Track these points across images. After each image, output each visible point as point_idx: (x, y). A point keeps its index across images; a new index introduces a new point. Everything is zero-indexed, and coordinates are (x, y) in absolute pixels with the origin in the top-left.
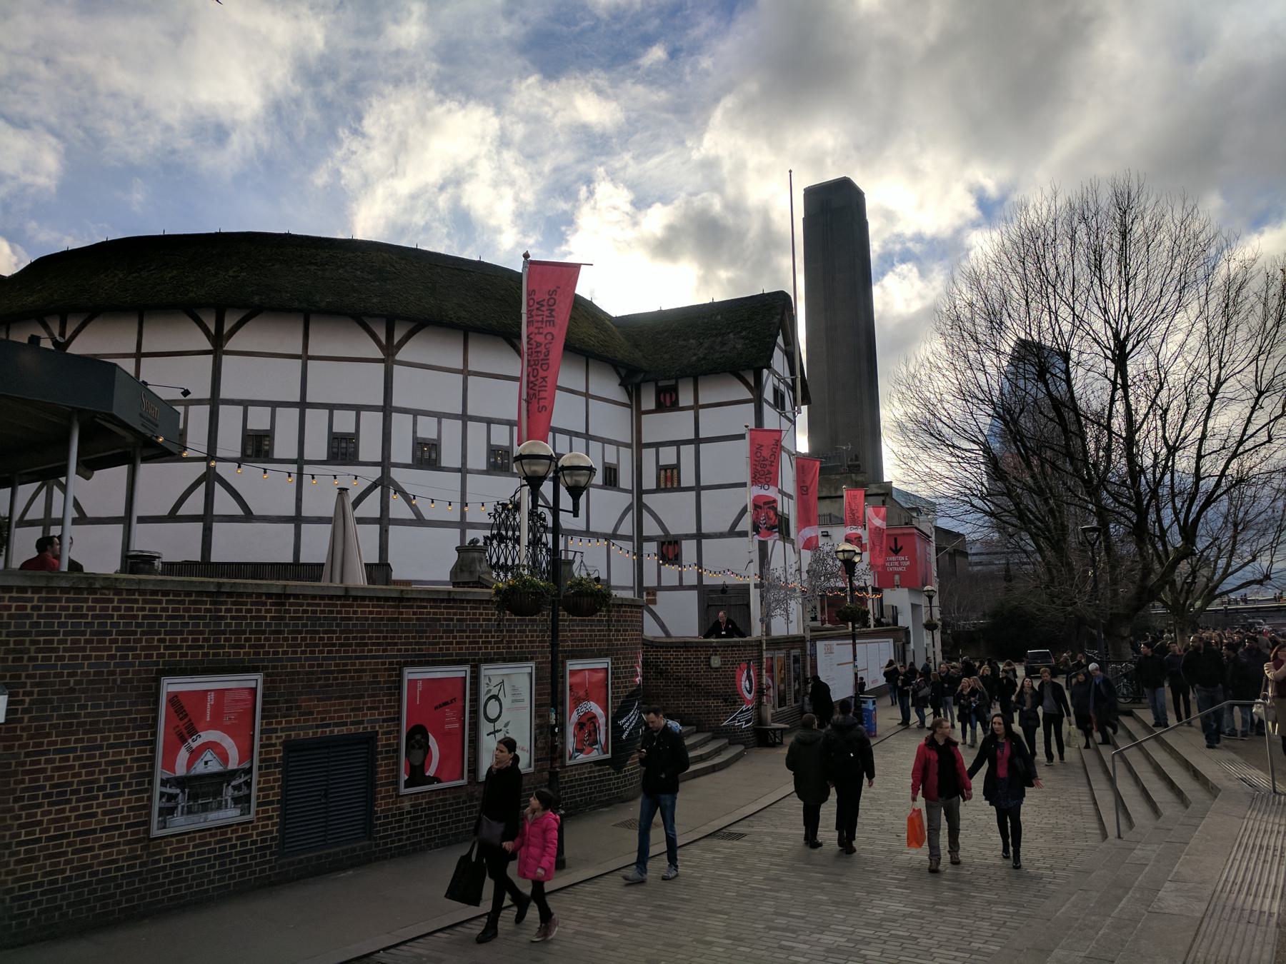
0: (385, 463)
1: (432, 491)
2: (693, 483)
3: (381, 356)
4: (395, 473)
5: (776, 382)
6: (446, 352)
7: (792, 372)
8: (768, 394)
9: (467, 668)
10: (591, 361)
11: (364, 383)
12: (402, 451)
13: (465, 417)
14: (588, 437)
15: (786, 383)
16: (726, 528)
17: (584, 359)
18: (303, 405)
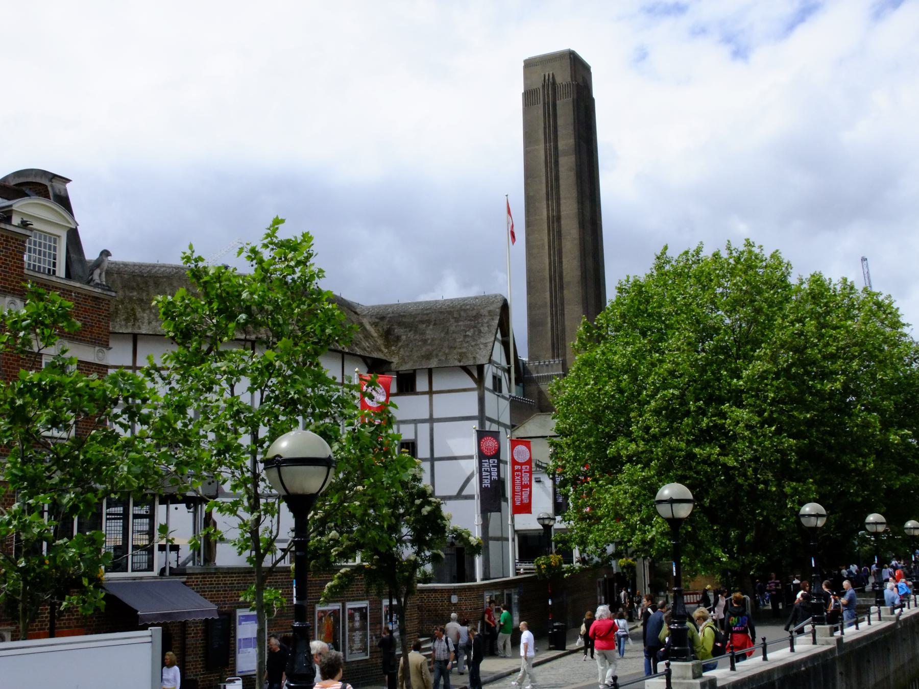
2: (428, 455)
5: (495, 370)
7: (508, 362)
8: (489, 383)
9: (340, 604)
10: (346, 356)
15: (504, 370)
16: (455, 493)
17: (340, 355)
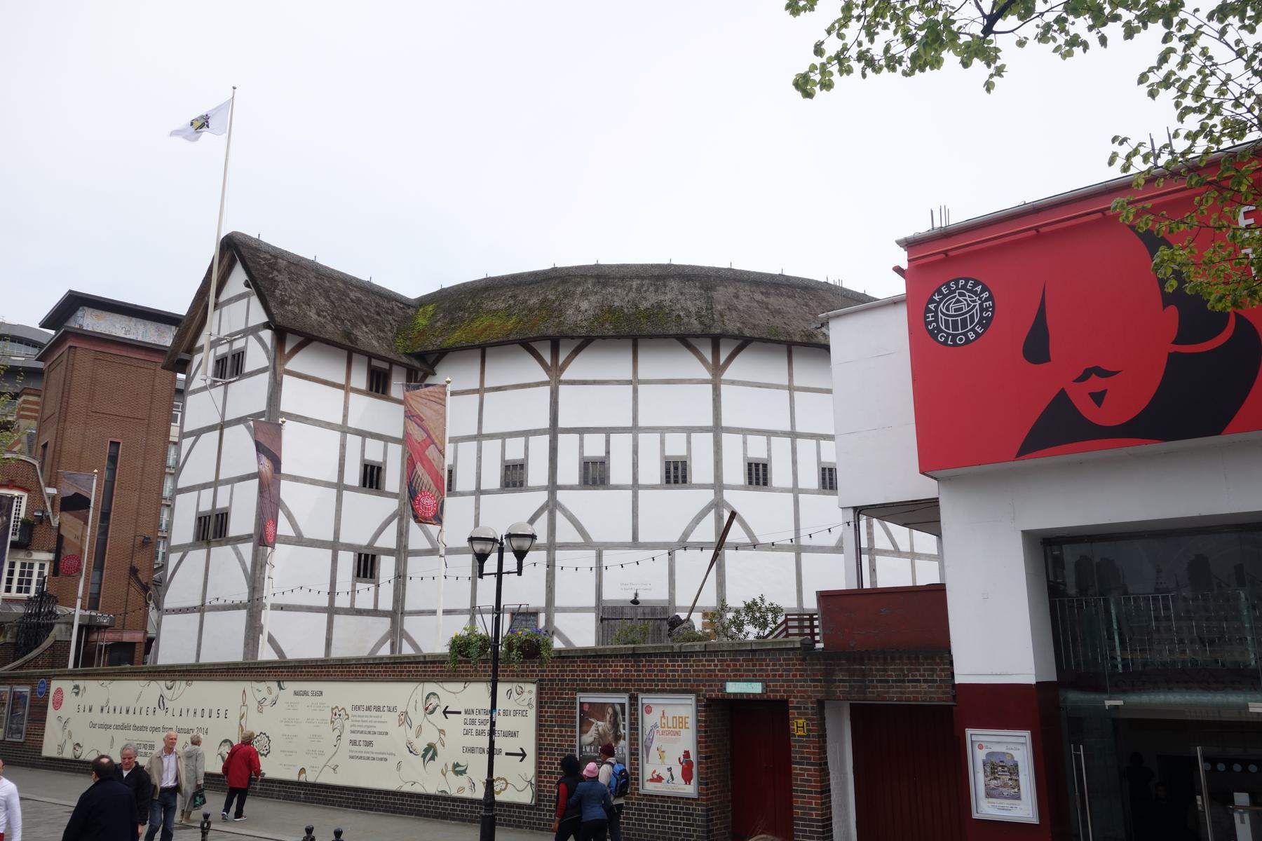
0: (553, 487)
1: (600, 512)
3: (546, 378)
4: (561, 496)
6: (615, 365)
11: (530, 408)
12: (569, 472)
13: (635, 429)
14: (793, 435)
17: (785, 347)
18: (480, 437)
